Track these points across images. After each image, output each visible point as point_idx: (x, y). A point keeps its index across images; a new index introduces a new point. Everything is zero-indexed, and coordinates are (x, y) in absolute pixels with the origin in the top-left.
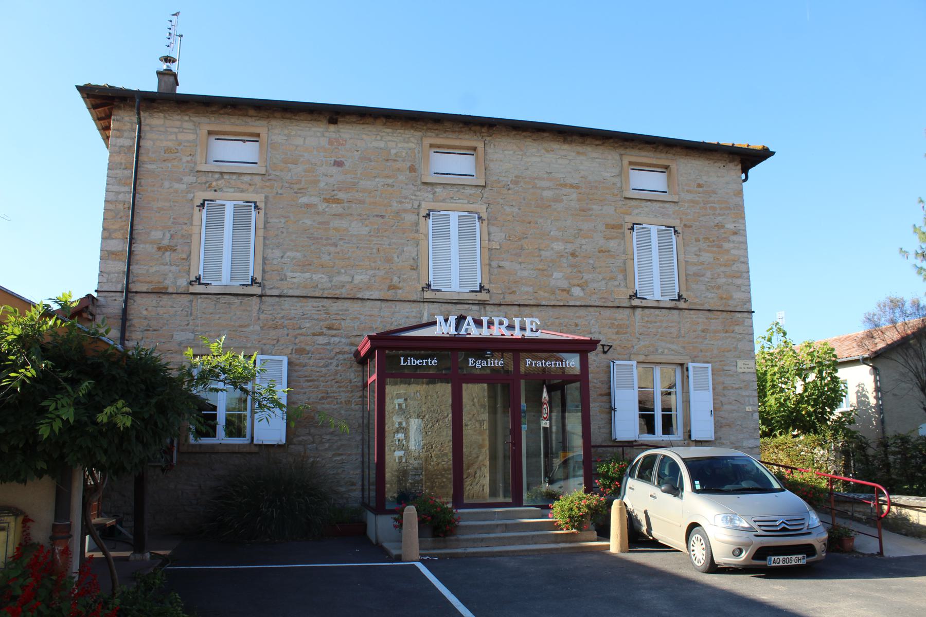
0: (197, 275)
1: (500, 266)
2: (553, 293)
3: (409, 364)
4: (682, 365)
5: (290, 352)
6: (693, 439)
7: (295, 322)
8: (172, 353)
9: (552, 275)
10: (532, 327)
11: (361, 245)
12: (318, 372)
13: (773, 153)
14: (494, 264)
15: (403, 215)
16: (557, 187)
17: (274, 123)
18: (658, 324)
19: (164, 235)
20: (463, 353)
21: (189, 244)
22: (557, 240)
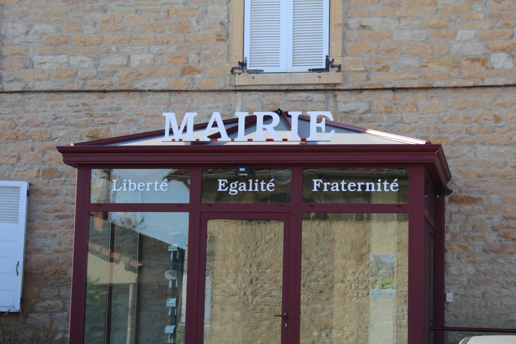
1: (364, 26)
5: (35, 174)
7: (43, 130)
9: (455, 35)
11: (142, 7)
14: (354, 23)
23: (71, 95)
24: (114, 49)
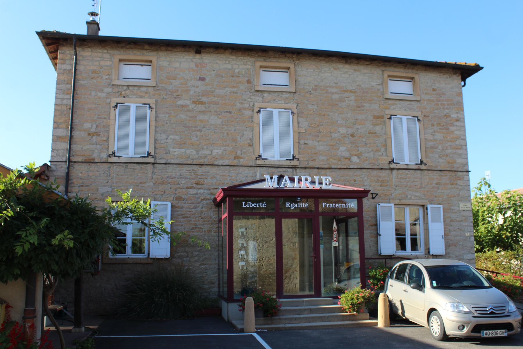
0: (113, 150)
2: (340, 160)
4: (423, 206)
5: (172, 199)
6: (431, 253)
7: (175, 180)
8: (98, 201)
9: (339, 149)
10: (326, 182)
12: (190, 212)
13: (482, 68)
14: (302, 142)
15: (244, 111)
16: (342, 92)
17: (161, 53)
18: (408, 179)
19: (92, 125)
20: (282, 199)
21: (108, 131)
22: (341, 126)
23: (187, 166)
24: (205, 147)
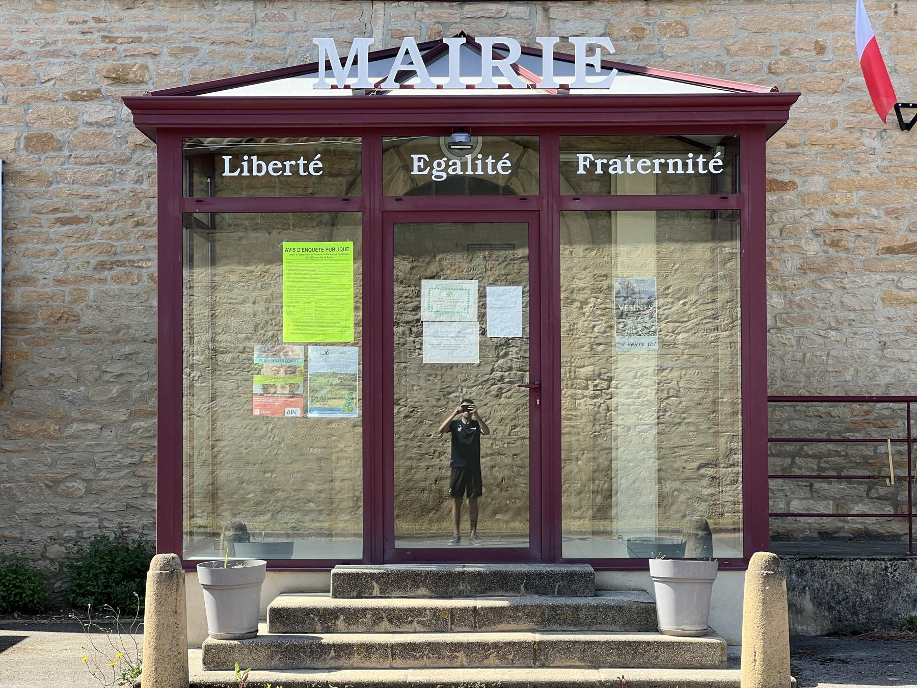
3: (245, 173)
7: (23, 64)
10: (590, 60)
12: (88, 197)
20: (480, 139)
